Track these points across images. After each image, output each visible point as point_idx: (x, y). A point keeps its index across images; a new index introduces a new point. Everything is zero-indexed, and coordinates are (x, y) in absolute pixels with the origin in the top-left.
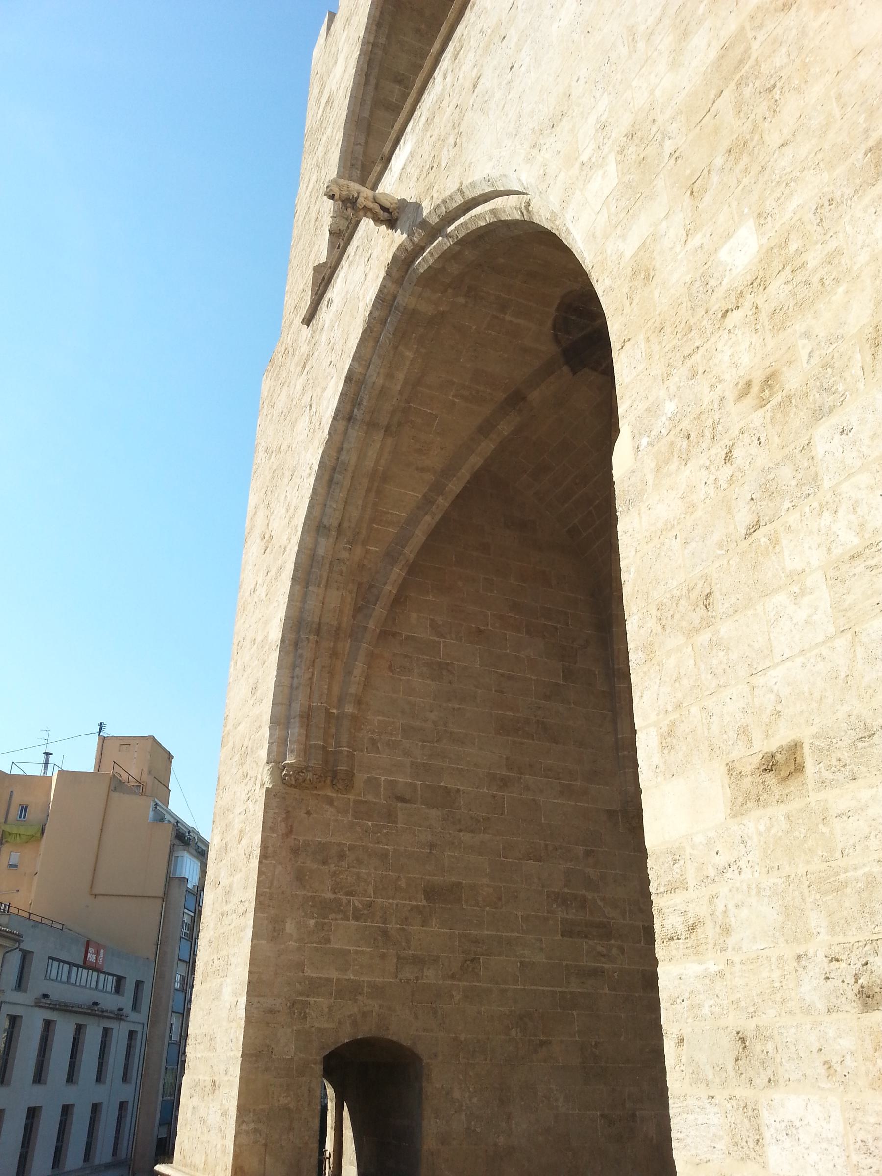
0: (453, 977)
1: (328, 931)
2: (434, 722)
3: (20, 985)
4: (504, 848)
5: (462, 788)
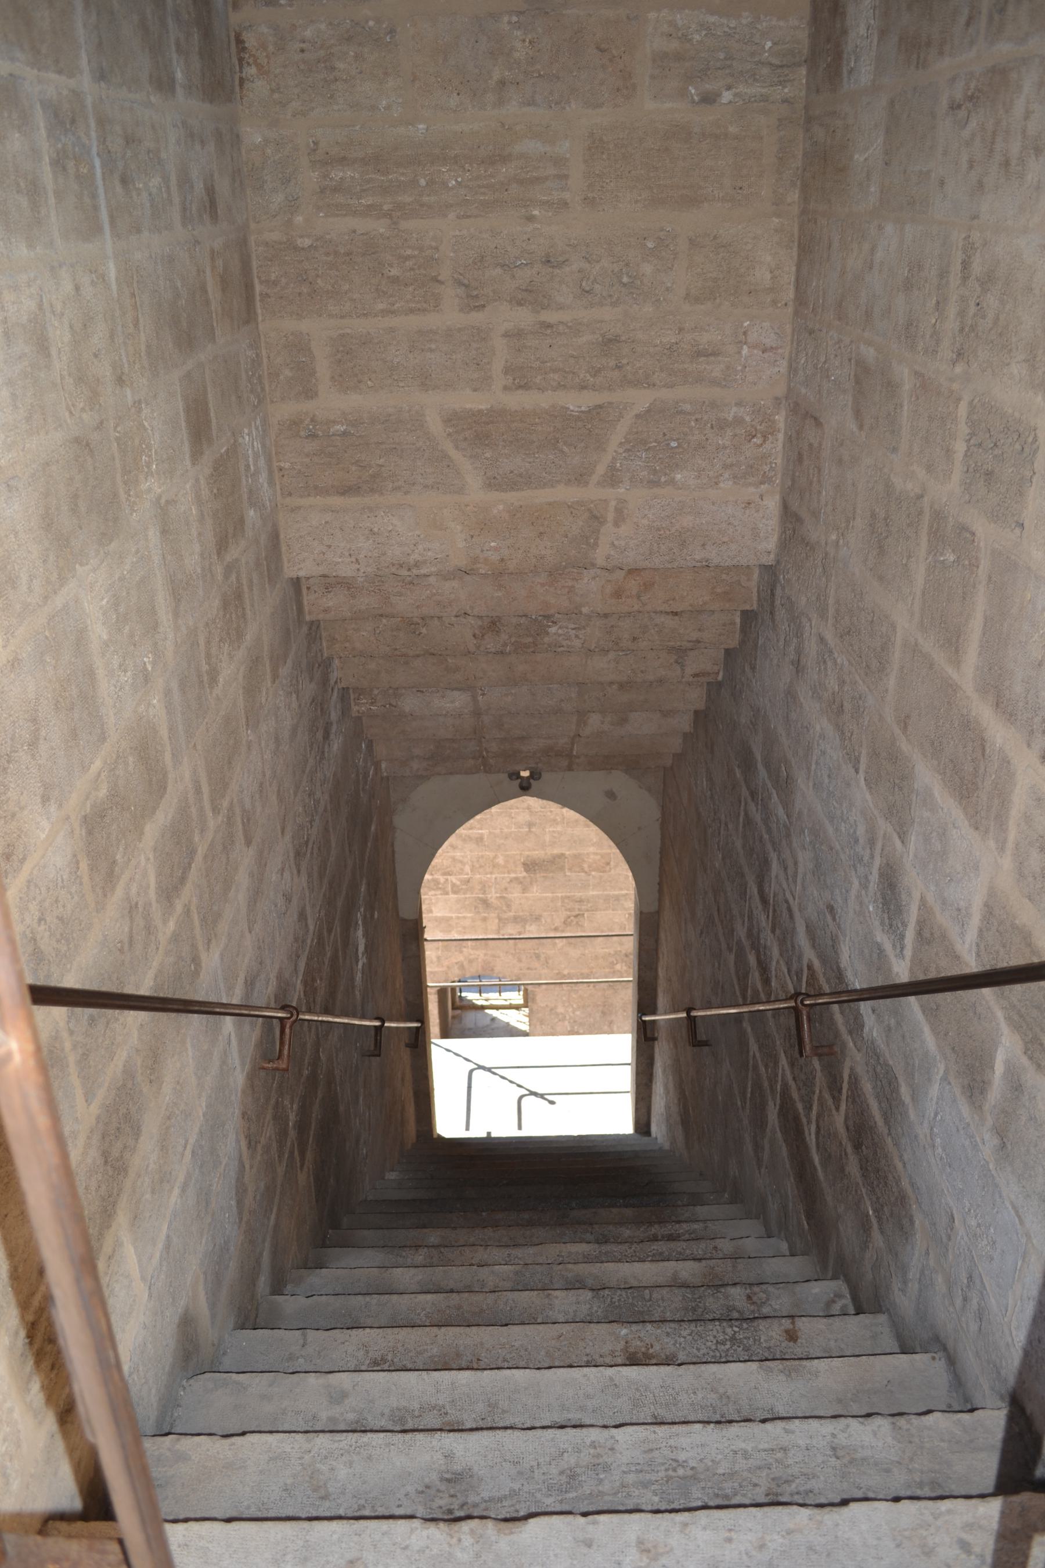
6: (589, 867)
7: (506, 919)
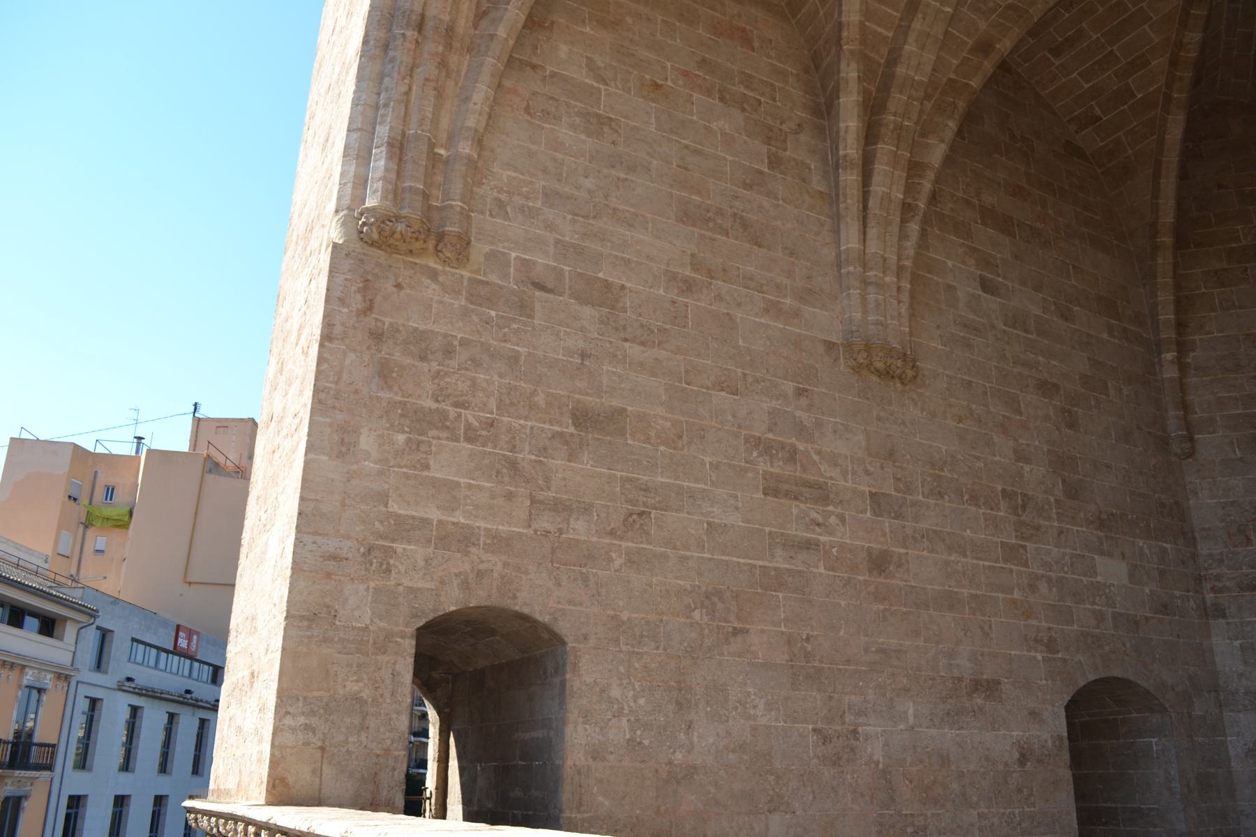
0: (612, 533)
1: (425, 452)
2: (589, 192)
3: (99, 665)
4: (687, 372)
5: (628, 285)
6: (658, 437)
7: (541, 502)
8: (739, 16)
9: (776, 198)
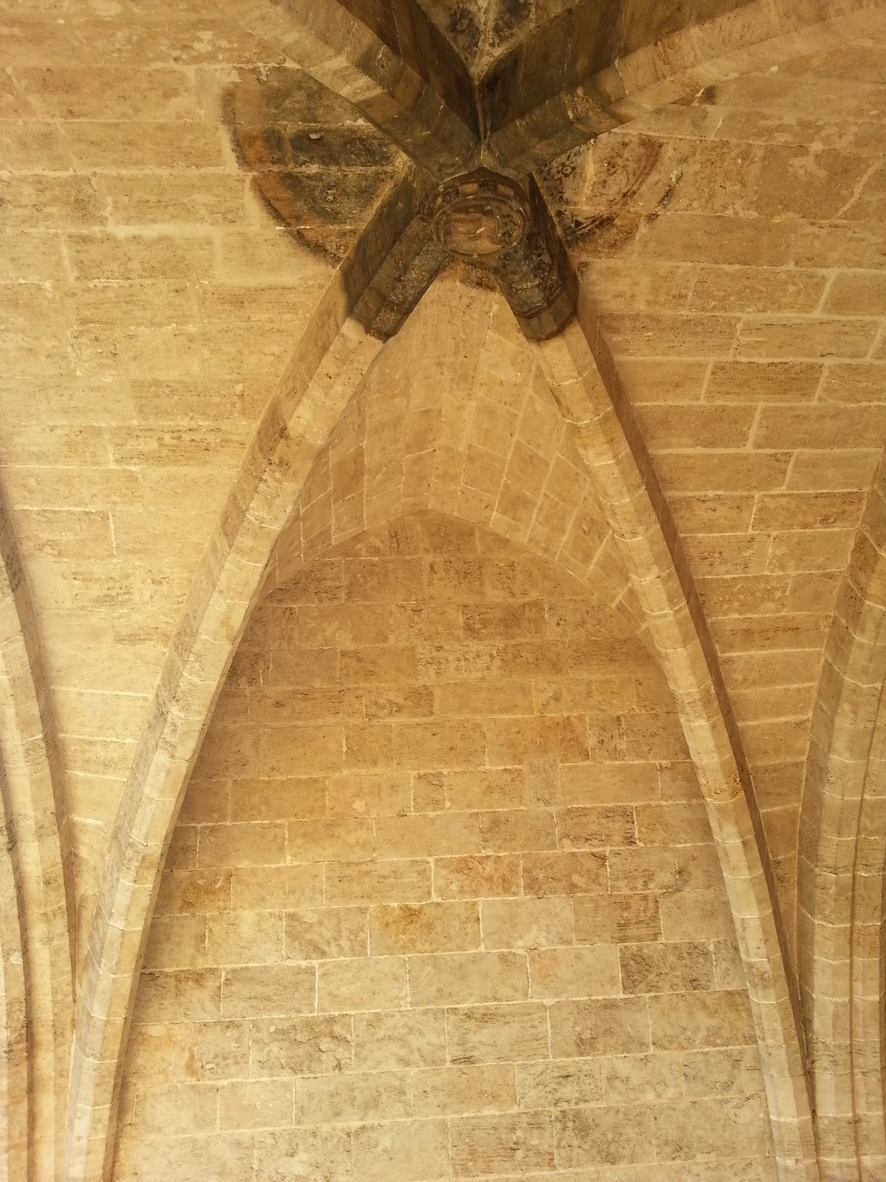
8: (557, 699)
9: (643, 1045)
